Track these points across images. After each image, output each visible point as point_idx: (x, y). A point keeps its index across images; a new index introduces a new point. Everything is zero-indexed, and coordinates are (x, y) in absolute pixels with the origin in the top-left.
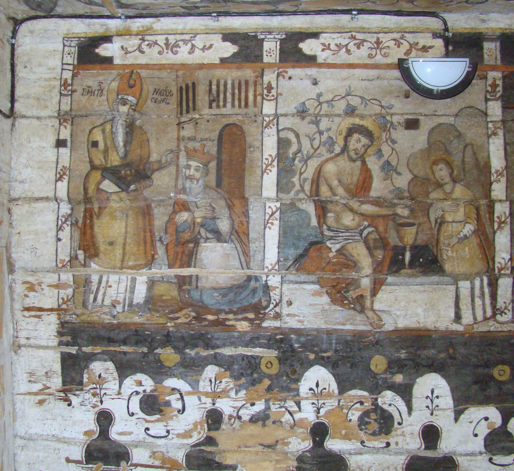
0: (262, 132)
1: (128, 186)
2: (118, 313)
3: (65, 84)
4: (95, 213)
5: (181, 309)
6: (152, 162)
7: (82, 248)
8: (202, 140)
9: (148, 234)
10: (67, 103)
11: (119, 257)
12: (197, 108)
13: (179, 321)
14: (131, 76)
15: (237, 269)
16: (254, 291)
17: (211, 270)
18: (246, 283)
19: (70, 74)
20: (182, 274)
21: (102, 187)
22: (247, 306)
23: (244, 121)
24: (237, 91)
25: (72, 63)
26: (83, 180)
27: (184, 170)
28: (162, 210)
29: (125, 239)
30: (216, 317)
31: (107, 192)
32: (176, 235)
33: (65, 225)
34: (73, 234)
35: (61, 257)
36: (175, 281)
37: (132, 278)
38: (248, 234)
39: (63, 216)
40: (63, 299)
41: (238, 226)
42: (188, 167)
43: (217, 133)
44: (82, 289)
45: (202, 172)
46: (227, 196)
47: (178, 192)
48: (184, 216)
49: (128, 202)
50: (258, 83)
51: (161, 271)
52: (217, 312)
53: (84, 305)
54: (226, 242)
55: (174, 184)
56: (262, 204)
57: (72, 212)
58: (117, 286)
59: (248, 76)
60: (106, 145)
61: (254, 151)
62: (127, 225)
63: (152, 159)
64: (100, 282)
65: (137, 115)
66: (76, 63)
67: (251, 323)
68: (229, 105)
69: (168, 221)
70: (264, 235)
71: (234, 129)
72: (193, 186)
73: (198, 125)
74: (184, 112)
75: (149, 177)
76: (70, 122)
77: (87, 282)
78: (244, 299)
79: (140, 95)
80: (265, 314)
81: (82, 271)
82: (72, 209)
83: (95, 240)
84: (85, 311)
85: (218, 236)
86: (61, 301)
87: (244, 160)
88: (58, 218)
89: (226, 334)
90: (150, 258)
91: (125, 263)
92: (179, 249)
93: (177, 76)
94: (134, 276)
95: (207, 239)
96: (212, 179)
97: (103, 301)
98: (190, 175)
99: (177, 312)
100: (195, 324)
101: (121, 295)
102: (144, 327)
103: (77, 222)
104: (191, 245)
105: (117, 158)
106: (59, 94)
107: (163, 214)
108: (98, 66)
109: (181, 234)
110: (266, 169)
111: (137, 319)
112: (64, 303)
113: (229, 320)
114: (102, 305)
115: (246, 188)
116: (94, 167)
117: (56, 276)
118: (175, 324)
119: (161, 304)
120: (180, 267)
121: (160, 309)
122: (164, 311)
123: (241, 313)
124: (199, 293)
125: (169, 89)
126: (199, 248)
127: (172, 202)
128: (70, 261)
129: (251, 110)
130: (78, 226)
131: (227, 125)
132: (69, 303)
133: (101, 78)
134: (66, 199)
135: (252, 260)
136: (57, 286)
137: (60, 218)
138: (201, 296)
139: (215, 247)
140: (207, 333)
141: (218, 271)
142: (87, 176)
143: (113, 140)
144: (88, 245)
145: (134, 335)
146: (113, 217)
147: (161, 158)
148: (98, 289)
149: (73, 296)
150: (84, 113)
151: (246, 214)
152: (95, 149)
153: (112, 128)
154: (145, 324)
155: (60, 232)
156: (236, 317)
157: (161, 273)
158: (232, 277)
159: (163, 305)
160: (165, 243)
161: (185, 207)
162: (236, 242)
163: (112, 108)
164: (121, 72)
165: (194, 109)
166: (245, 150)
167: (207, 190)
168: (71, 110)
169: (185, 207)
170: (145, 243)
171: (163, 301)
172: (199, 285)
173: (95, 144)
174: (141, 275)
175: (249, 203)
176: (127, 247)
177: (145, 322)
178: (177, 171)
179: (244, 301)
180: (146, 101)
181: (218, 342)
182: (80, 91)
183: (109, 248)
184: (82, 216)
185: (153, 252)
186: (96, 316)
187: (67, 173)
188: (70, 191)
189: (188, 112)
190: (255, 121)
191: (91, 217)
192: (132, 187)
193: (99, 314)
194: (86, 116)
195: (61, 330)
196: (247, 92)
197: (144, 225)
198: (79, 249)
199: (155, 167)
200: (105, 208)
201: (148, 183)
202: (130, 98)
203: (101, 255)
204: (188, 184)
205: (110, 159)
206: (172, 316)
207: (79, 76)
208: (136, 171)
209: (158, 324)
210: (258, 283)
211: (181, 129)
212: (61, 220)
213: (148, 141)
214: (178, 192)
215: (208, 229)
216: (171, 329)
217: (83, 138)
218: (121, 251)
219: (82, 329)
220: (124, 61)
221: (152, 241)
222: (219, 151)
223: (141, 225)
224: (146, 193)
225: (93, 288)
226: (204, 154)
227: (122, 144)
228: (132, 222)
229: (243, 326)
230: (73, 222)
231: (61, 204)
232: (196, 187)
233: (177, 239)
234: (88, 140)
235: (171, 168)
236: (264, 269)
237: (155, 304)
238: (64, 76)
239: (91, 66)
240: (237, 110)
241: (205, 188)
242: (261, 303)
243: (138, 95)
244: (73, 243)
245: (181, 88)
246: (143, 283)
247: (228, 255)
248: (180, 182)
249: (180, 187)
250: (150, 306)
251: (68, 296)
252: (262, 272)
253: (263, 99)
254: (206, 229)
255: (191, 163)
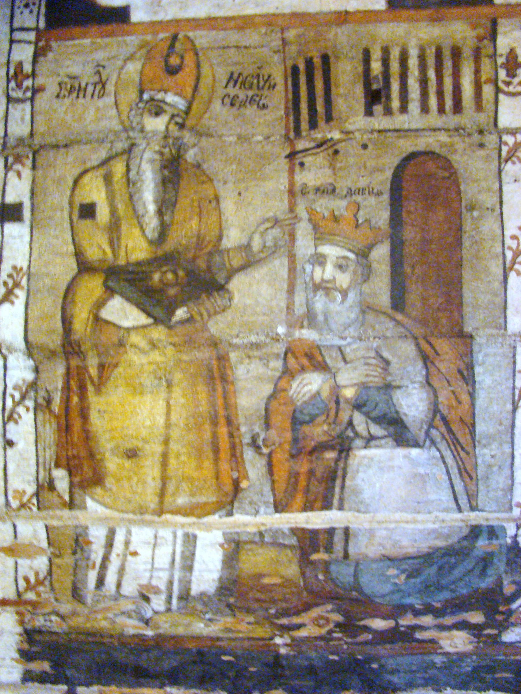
0: (500, 172)
1: (171, 312)
2: (156, 612)
3: (17, 75)
4: (90, 377)
5: (307, 607)
6: (228, 251)
7: (64, 462)
8: (350, 192)
9: (223, 430)
10: (23, 119)
11: (152, 484)
12: (335, 114)
13: (303, 633)
14: (172, 47)
15: (446, 510)
16: (486, 562)
17: (380, 516)
18: (465, 543)
19: (30, 50)
20: (310, 526)
21: (106, 314)
22: (469, 596)
23: (452, 145)
24: (432, 74)
25: (33, 25)
26: (60, 301)
27: (308, 268)
28: (256, 368)
29: (166, 441)
30: (391, 623)
31: (119, 327)
32: (293, 430)
33: (21, 410)
34: (40, 428)
35: (15, 483)
36: (293, 541)
37: (187, 536)
38: (473, 425)
39: (15, 388)
40: (27, 579)
41: (450, 407)
42: (320, 260)
43: (389, 174)
44: (68, 560)
45: (355, 273)
46: (418, 331)
47: (294, 323)
48: (310, 384)
49: (170, 350)
50: (483, 52)
51: (259, 519)
52: (398, 611)
53: (76, 594)
54: (416, 445)
55: (283, 305)
56: (506, 350)
57: (36, 378)
58: (150, 552)
59: (459, 36)
60: (113, 212)
61: (481, 217)
62: (168, 405)
63: (227, 243)
64: (110, 544)
65: (188, 137)
66: (42, 24)
67: (475, 636)
68: (414, 107)
69: (272, 397)
70: (513, 426)
71: (431, 166)
72: (335, 307)
73: (339, 157)
74: (304, 125)
75: (221, 288)
76: (29, 163)
77: (80, 542)
78: (460, 579)
79: (196, 89)
80: (510, 613)
81: (64, 518)
82: (36, 370)
83: (92, 443)
84: (79, 608)
85: (398, 431)
86: (22, 584)
87: (459, 243)
88: (4, 393)
89: (416, 660)
90: (229, 488)
91: (168, 499)
92: (303, 467)
93: (283, 40)
94: (190, 530)
95: (370, 440)
96: (381, 289)
97: (119, 585)
98: (323, 281)
99: (297, 613)
100: (340, 639)
101: (161, 574)
102: (220, 647)
103: (49, 401)
104: (330, 455)
105: (144, 244)
106: (4, 100)
107: (260, 379)
108: (95, 29)
109: (306, 429)
110: (514, 263)
111: (200, 628)
112: (29, 587)
113: (422, 628)
114: (118, 596)
115: (467, 310)
116: (85, 267)
117: (8, 528)
118: (293, 639)
119: (258, 595)
120: (305, 509)
121: (256, 606)
122: (267, 609)
123: (453, 613)
124: (352, 570)
125: (265, 72)
126: (350, 461)
127: (280, 348)
128: (37, 494)
129: (469, 117)
130: (51, 411)
131: (411, 157)
132: (41, 589)
133: (100, 56)
134: (22, 345)
135: (481, 487)
136: (12, 551)
137: (9, 390)
138: (356, 575)
139: (391, 459)
140: (369, 660)
141: (398, 516)
142: (70, 289)
143: (131, 199)
144: (78, 460)
145: (194, 662)
146: (138, 390)
147: (251, 239)
148: (106, 559)
149: (50, 572)
150: (61, 138)
151: (467, 374)
152: (88, 222)
153: (128, 170)
154: (219, 639)
155: (11, 426)
156: (440, 620)
157: (256, 525)
158: (434, 531)
159: (263, 597)
160: (265, 451)
161: (313, 359)
162: (443, 446)
163: (127, 123)
164: (149, 38)
165: (329, 118)
166: (460, 216)
167: (370, 317)
168: (32, 134)
169: (313, 359)
170: (216, 451)
171: (265, 588)
172: (351, 550)
173: (88, 211)
174: (209, 528)
175: (476, 348)
176: (173, 462)
177: (221, 635)
178: (292, 270)
179: (461, 584)
180: (210, 102)
181: (395, 679)
182: (52, 88)
183: (128, 464)
184: (60, 385)
185: (235, 475)
186: (105, 619)
187: (24, 282)
188: (31, 326)
189: (313, 125)
190: (482, 146)
191: (83, 388)
192: (181, 313)
193: (110, 615)
194: (66, 146)
195: (26, 646)
196: (456, 75)
197: (213, 405)
198: (58, 465)
199: (236, 262)
200: (116, 365)
201: (219, 300)
202: (170, 98)
203: (109, 482)
204: (320, 303)
205: (123, 242)
206: (284, 621)
207: (50, 55)
208: (189, 273)
209: (252, 639)
210: (495, 542)
211: (297, 168)
212: (13, 396)
213: (217, 199)
214: (294, 323)
215: (374, 414)
216: (283, 651)
217: (58, 199)
218: (156, 472)
219: (75, 645)
220: (156, 13)
221: (233, 447)
222: (396, 220)
223: (204, 407)
224: (217, 327)
225: (93, 556)
226: (357, 226)
227: (152, 208)
228: (182, 400)
229: (457, 642)
230: (41, 401)
231: (12, 360)
232: (341, 311)
233: (295, 440)
234: (71, 204)
235: (277, 262)
236: (511, 509)
237: (242, 595)
238: (16, 57)
239: (77, 30)
240: (434, 119)
241: (363, 312)
242: (501, 589)
243: (189, 91)
244: (41, 453)
245: (295, 70)
246: (213, 545)
247: (423, 478)
248: (299, 298)
249: (300, 309)
250: (232, 600)
251: (37, 574)
252: (505, 515)
253: (498, 90)
254: (367, 415)
255: (326, 249)
